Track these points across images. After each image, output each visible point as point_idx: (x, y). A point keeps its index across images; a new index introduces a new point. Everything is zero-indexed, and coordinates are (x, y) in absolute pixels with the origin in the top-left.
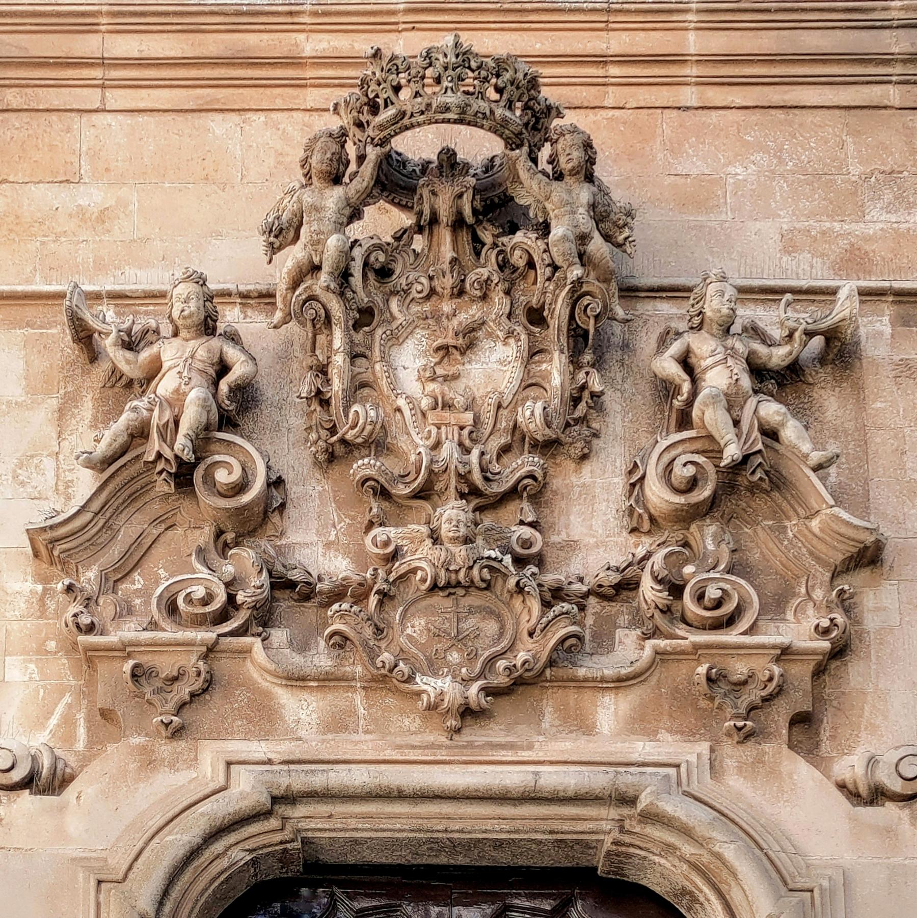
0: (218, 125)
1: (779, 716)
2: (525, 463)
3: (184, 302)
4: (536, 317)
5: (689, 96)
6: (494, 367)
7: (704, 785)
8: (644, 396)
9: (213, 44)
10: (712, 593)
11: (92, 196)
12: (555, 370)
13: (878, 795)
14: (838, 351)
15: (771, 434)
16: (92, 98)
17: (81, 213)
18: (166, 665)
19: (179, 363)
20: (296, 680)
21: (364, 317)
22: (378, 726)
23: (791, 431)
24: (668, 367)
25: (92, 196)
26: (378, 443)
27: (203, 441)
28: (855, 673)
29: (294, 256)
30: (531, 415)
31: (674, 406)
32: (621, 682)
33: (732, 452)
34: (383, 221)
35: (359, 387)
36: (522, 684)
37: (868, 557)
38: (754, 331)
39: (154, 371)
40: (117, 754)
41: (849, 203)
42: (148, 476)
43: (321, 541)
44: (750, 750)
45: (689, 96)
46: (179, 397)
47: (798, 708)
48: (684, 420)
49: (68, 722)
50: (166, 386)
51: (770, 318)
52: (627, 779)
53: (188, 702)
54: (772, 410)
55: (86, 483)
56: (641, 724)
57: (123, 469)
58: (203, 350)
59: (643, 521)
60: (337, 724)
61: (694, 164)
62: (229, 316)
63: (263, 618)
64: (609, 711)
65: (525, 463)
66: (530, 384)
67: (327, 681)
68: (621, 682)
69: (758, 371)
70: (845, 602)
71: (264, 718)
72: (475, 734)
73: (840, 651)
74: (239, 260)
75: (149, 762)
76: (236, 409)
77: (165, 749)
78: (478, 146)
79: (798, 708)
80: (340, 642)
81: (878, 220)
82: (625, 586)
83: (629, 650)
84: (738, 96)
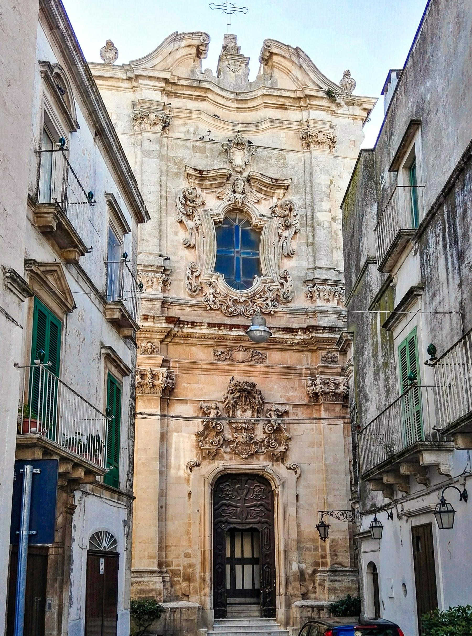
0: (215, 377)
2: (252, 426)
5: (270, 376)
6: (248, 414)
7: (271, 467)
9: (215, 367)
11: (200, 386)
12: (255, 415)
13: (290, 469)
15: (279, 424)
16: (200, 373)
17: (199, 388)
20: (226, 453)
22: (235, 459)
23: (281, 425)
25: (200, 386)
28: (288, 452)
36: (252, 455)
37: (290, 439)
41: (287, 391)
44: (276, 463)
45: (270, 376)
47: (281, 458)
49: (199, 457)
53: (213, 455)
56: (265, 459)
57: (207, 427)
58: (216, 411)
59: (264, 433)
60: (231, 459)
65: (252, 426)
66: (253, 415)
67: (230, 453)
69: (278, 415)
70: (287, 445)
71: (222, 458)
75: (209, 463)
77: (211, 461)
79: (281, 458)
84: (276, 377)
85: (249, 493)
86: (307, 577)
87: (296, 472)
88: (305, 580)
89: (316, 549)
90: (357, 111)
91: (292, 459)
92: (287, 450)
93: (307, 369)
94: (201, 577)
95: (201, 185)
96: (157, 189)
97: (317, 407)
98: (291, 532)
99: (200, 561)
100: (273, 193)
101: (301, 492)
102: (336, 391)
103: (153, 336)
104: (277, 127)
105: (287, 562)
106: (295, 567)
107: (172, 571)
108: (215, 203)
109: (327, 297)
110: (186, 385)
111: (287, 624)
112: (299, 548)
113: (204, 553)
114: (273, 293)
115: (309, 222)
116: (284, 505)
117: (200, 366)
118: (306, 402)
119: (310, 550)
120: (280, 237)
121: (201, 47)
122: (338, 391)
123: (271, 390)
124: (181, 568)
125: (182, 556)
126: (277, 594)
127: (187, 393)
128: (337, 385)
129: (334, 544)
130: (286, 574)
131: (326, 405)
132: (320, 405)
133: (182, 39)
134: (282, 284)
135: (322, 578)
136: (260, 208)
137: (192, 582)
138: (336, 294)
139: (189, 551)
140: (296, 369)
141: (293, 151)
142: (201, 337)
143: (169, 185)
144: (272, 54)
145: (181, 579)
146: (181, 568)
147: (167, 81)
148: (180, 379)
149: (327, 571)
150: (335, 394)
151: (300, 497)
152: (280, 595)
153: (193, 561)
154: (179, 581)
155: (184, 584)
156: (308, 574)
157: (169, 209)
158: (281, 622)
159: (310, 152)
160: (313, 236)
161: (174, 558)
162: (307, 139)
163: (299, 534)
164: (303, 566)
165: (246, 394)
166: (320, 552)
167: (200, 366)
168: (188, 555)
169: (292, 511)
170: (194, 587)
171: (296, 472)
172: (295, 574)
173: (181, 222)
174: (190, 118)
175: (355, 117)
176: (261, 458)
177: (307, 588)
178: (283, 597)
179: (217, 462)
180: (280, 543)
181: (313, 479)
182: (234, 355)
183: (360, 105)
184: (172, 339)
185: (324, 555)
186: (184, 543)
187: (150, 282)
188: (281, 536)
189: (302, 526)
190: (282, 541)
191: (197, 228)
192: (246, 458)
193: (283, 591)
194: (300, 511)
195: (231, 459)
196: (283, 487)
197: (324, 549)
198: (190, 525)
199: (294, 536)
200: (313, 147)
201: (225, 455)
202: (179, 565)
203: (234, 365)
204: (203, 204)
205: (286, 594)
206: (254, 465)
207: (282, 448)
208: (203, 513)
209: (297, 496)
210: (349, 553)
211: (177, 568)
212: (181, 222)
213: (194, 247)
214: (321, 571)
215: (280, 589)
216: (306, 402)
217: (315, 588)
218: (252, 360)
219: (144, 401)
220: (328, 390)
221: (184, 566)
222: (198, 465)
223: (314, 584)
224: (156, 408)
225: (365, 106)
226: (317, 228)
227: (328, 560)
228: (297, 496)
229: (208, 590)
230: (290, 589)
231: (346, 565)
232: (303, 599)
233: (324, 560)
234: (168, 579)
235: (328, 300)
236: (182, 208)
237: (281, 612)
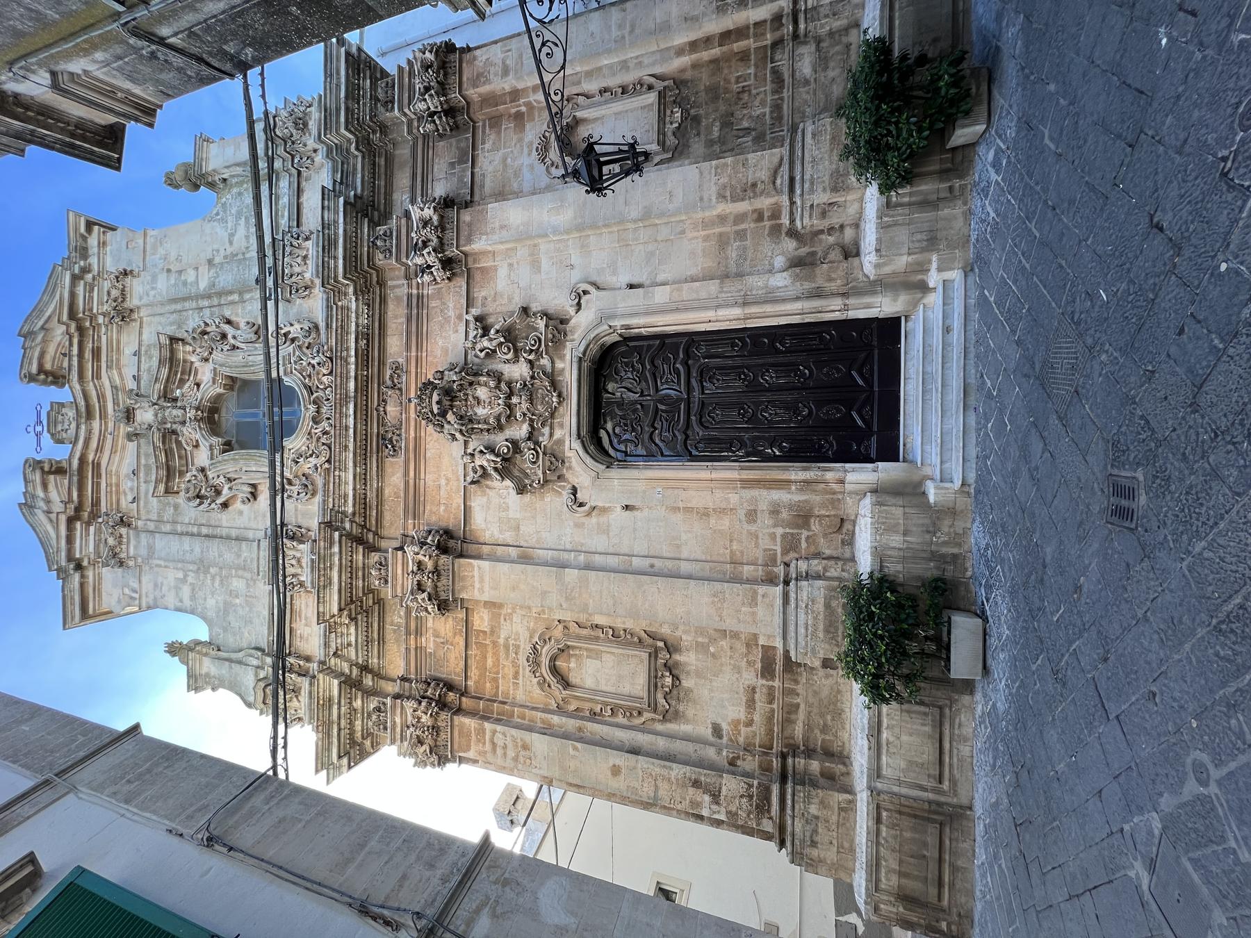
0: (428, 455)
1: (561, 327)
2: (503, 385)
3: (467, 459)
4: (471, 384)
6: (482, 393)
7: (577, 343)
8: (488, 362)
9: (412, 456)
11: (443, 482)
13: (579, 304)
14: (479, 319)
15: (497, 332)
18: (548, 464)
19: (480, 461)
20: (551, 435)
21: (471, 421)
22: (563, 416)
23: (497, 327)
24: (482, 355)
26: (498, 418)
27: (497, 455)
28: (550, 312)
29: (458, 435)
30: (492, 384)
31: (491, 354)
32: (553, 362)
33: (502, 340)
34: (450, 417)
35: (486, 422)
38: (475, 337)
39: (482, 467)
40: (568, 475)
41: (447, 320)
42: (506, 467)
43: (520, 431)
47: (558, 323)
48: (494, 351)
50: (485, 464)
51: (472, 334)
53: (555, 460)
54: (492, 331)
55: (508, 483)
56: (562, 358)
57: (504, 472)
58: (477, 455)
59: (516, 360)
60: (561, 426)
61: (439, 353)
62: (469, 451)
63: (537, 443)
64: (559, 365)
65: (503, 385)
66: (486, 385)
67: (552, 428)
68: (553, 362)
69: (483, 336)
71: (560, 442)
72: (565, 394)
73: (546, 314)
74: (457, 448)
75: (570, 468)
76: (491, 449)
78: (435, 398)
79: (558, 323)
80: (543, 425)
81: (451, 313)
82: (530, 362)
83: (545, 361)
86: (804, 251)
87: (585, 292)
88: (813, 254)
89: (741, 235)
90: (93, 241)
91: (561, 302)
92: (545, 314)
93: (410, 286)
94: (801, 490)
95: (182, 474)
96: (187, 539)
97: (470, 260)
98: (703, 295)
99: (764, 492)
100: (185, 361)
101: (625, 279)
102: (436, 223)
103: (360, 565)
104: (118, 360)
105: (771, 298)
106: (781, 281)
107: (785, 552)
108: (203, 452)
109: (299, 260)
110: (442, 508)
111: (924, 288)
112: (740, 275)
113: (747, 484)
114: (305, 354)
115: (215, 301)
116: (647, 313)
117: (411, 482)
118: (461, 282)
119: (745, 248)
120: (234, 348)
121: (46, 469)
122: (435, 218)
123: (445, 351)
124: (780, 531)
125: (753, 528)
126: (844, 317)
127: (454, 505)
128: (426, 223)
129: (728, 194)
130: (798, 298)
131: (462, 242)
132: (466, 255)
133: (34, 496)
134: (293, 340)
135: (806, 214)
136: (206, 379)
137: (811, 509)
138: (295, 243)
139: (741, 513)
140: (409, 305)
141: (140, 334)
142: (362, 478)
143: (187, 521)
144: (41, 370)
145: (805, 533)
146: (780, 531)
147: (70, 521)
148: (434, 519)
149: (792, 203)
150: (442, 226)
151: (635, 281)
152: (846, 308)
153: (763, 506)
154: (808, 538)
155: (815, 526)
156: (796, 249)
157: (213, 523)
158: (915, 304)
159: (138, 308)
160: (231, 293)
161: (757, 545)
162: (123, 314)
163: (706, 277)
164: (779, 261)
165: (448, 399)
166: (748, 225)
167: (411, 482)
168: (752, 516)
169: (661, 295)
170: (823, 505)
171: (585, 292)
172: (797, 278)
173: (225, 505)
174: (118, 485)
175: (102, 244)
176: (559, 365)
177: (831, 247)
178: (852, 301)
179: (568, 453)
180: (727, 318)
181: (596, 256)
182: (394, 422)
183: (84, 238)
184: (369, 530)
185: (755, 216)
186: (725, 523)
187: (294, 562)
188: (710, 314)
189: (693, 271)
190: (722, 313)
191: (230, 480)
192: (559, 396)
193: (837, 303)
194: (661, 277)
195: (561, 426)
196: (613, 316)
197: (740, 218)
198: (688, 510)
199: (713, 287)
200: (132, 302)
201: (555, 437)
202: (773, 537)
203: (408, 419)
204: (203, 470)
205: (844, 295)
206: (570, 377)
207: (541, 324)
208: (664, 483)
209: (631, 286)
210: (750, 156)
211: (779, 540)
212: (225, 505)
213: (254, 486)
214: (792, 221)
215: (833, 310)
216: (461, 282)
217: (831, 230)
218: (400, 389)
219: (464, 588)
220: (435, 240)
221: (775, 526)
222: (574, 491)
223: (822, 232)
224: (473, 567)
225: (82, 230)
226: (218, 288)
227: (765, 203)
228: (631, 286)
229: (829, 476)
230: (833, 286)
231: (776, 160)
232: (858, 254)
233: (766, 215)
234: (803, 566)
235: (305, 257)
236: (206, 502)
237: (882, 306)
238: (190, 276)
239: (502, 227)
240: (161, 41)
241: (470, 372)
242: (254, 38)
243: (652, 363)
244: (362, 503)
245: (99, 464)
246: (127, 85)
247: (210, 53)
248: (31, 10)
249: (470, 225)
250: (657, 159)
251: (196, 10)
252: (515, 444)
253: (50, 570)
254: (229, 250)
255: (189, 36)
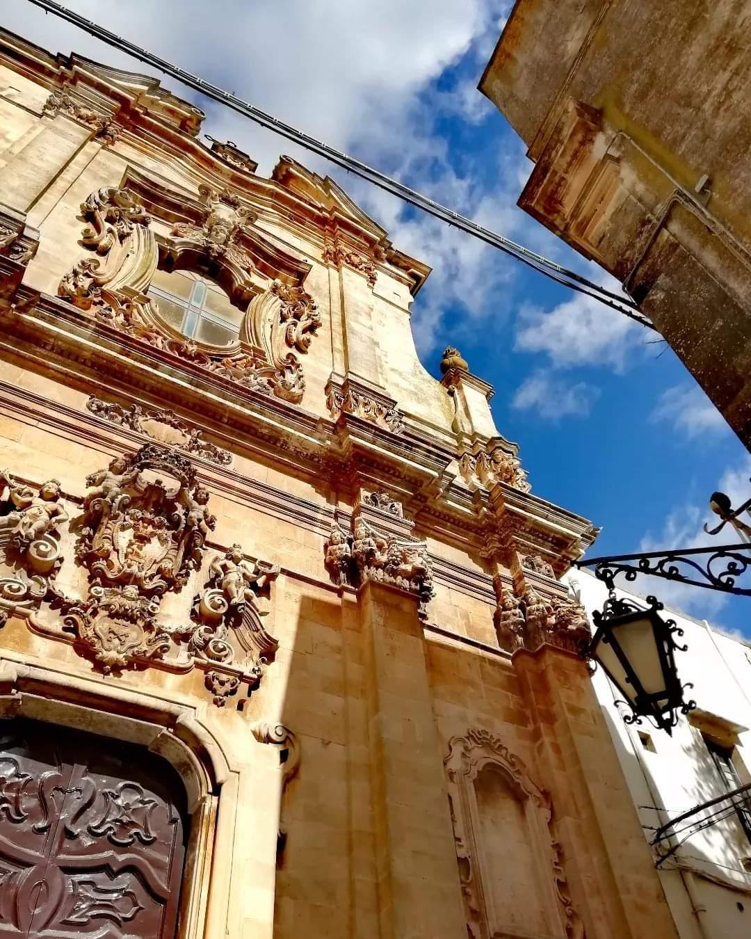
10: (220, 646)
16: (34, 422)
17: (15, 451)
27: (40, 533)
29: (94, 490)
46: (35, 517)
50: (33, 510)
52: (174, 708)
56: (183, 688)
59: (197, 616)
60: (55, 655)
64: (171, 679)
85: (91, 812)
131: (377, 591)
144: (289, 176)
183: (406, 269)
191: (122, 237)
204: (145, 222)
238: (363, 319)
239: (393, 648)
240: (664, 225)
241: (190, 541)
242: (678, 295)
243: (129, 868)
244: (33, 338)
245: (181, 158)
246: (610, 210)
247: (654, 264)
248: (684, 137)
249: (398, 608)
250: (475, 928)
251: (703, 246)
252: (50, 571)
253: (73, 54)
254: (386, 367)
255: (672, 245)
